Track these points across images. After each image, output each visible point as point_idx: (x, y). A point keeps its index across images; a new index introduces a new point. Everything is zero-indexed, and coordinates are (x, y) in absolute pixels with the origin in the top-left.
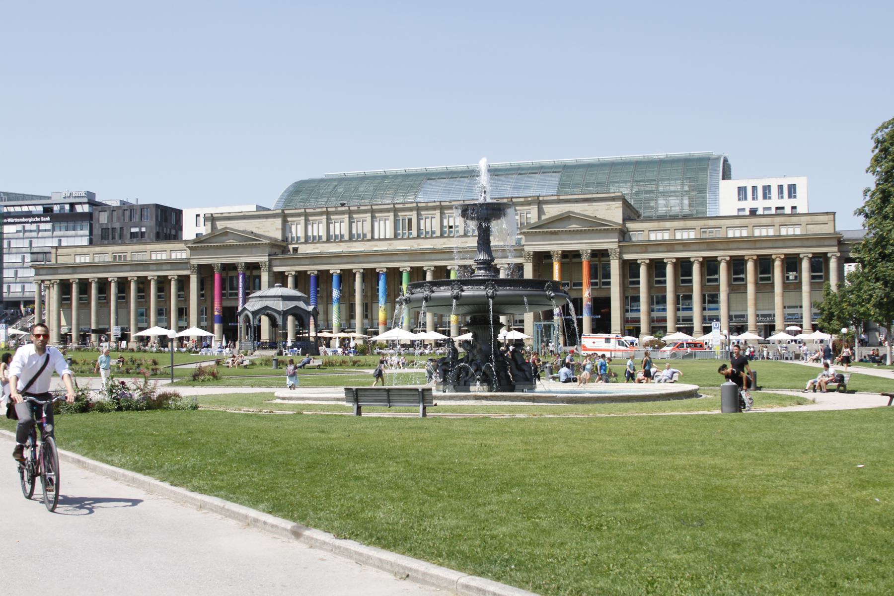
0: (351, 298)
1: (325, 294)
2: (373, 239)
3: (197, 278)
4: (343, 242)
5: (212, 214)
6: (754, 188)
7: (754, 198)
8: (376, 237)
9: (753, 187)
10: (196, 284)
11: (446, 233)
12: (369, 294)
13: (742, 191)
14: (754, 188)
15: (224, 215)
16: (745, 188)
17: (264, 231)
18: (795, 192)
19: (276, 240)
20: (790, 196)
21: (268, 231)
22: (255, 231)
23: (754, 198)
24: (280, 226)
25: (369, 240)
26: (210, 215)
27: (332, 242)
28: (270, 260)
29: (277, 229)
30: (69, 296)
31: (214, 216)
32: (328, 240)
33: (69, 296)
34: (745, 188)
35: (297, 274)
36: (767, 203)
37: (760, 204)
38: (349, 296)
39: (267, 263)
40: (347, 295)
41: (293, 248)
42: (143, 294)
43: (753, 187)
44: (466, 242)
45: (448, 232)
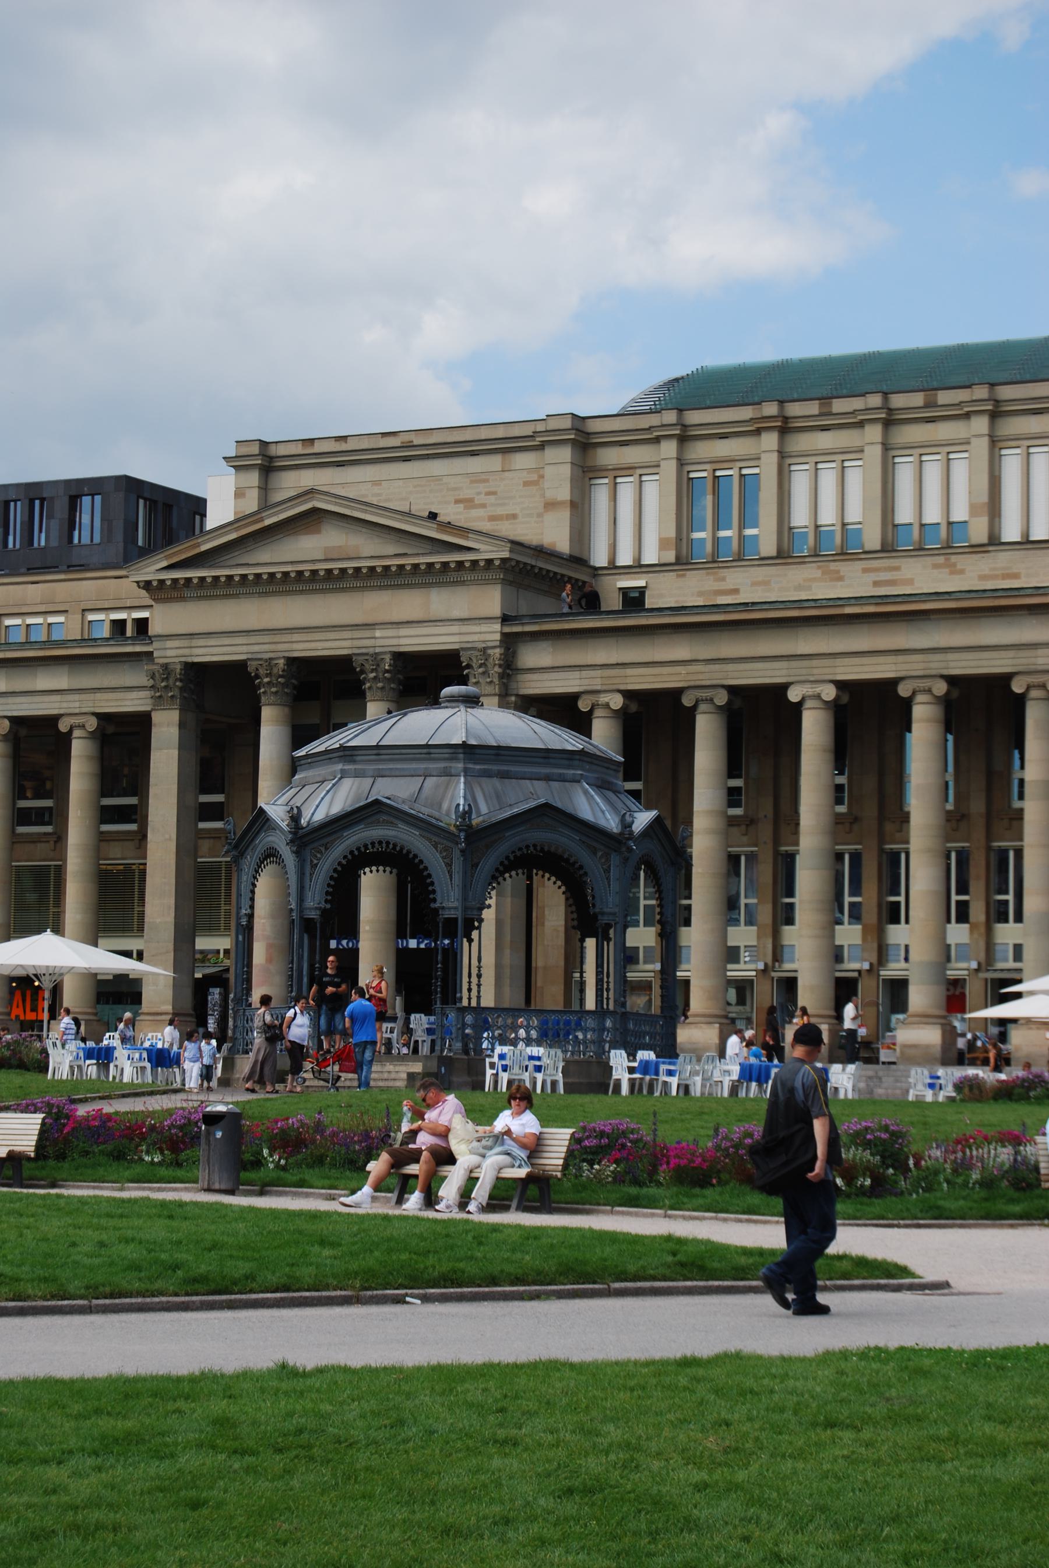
0: (889, 827)
1: (767, 809)
2: (994, 541)
3: (182, 725)
4: (854, 557)
5: (264, 444)
8: (1011, 532)
12: (977, 806)
15: (318, 448)
17: (493, 518)
19: (550, 554)
22: (449, 513)
24: (564, 493)
25: (977, 549)
26: (255, 449)
27: (801, 561)
28: (510, 642)
29: (551, 505)
30: (133, 801)
31: (273, 451)
32: (783, 555)
33: (133, 801)
35: (634, 708)
38: (882, 818)
40: (870, 810)
41: (625, 592)
42: (219, 798)
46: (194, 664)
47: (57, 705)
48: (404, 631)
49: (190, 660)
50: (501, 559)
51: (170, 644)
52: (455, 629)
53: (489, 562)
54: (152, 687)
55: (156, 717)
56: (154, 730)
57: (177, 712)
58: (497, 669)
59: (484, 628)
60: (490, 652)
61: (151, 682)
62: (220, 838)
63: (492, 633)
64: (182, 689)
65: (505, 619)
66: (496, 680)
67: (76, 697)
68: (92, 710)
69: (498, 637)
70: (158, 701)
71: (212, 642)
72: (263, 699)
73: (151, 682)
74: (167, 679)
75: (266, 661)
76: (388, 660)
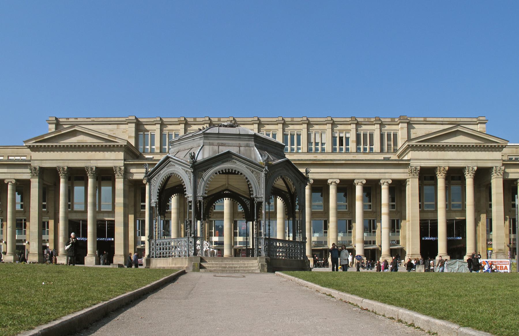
39: (123, 168)
46: (42, 167)
47: (4, 176)
49: (41, 166)
50: (124, 145)
52: (112, 162)
53: (121, 146)
54: (31, 172)
55: (32, 180)
56: (32, 184)
57: (38, 179)
58: (123, 172)
59: (119, 162)
60: (121, 167)
61: (31, 171)
62: (45, 213)
63: (121, 164)
64: (39, 173)
65: (125, 160)
66: (123, 175)
67: (9, 174)
68: (14, 178)
69: (123, 164)
70: (33, 176)
72: (61, 177)
73: (31, 171)
74: (35, 171)
75: (62, 167)
76: (95, 168)
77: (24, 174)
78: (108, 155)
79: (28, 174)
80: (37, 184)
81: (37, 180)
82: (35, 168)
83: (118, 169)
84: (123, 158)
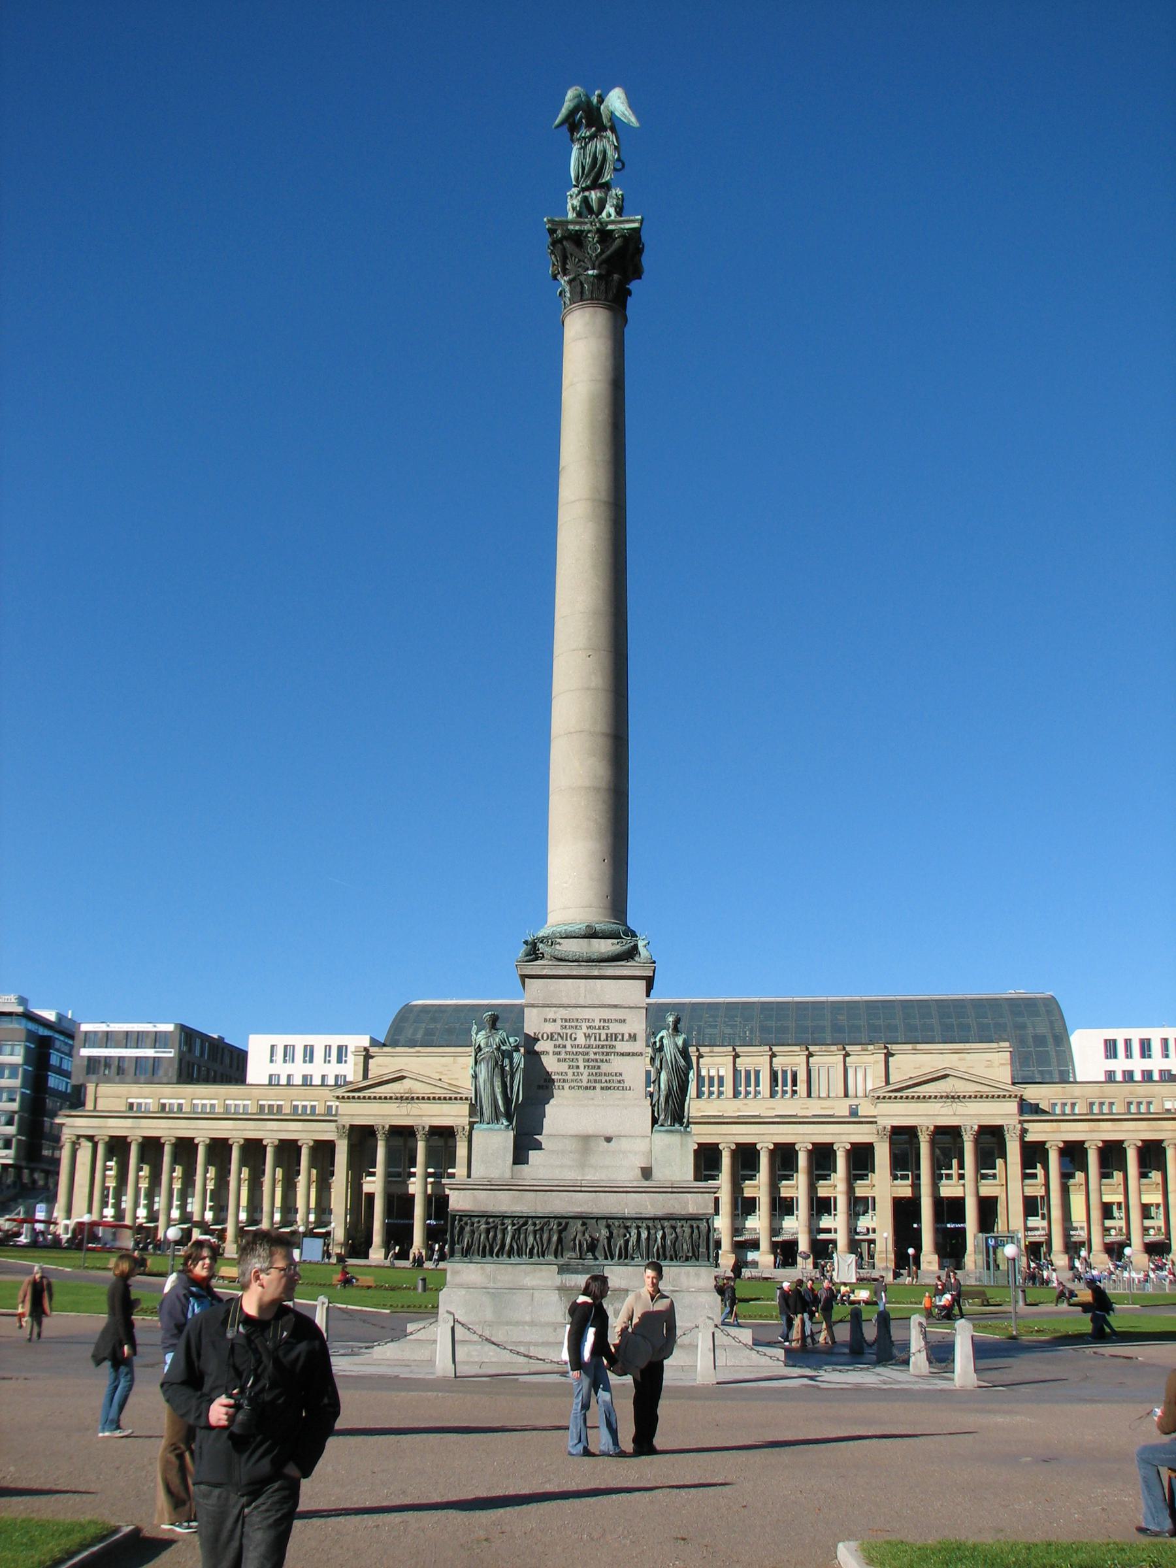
6: (1128, 1042)
7: (1129, 1055)
9: (1126, 1041)
10: (345, 1156)
11: (750, 1093)
13: (1110, 1049)
14: (1128, 1042)
16: (1114, 1041)
18: (1149, 1050)
20: (1143, 1056)
21: (457, 1079)
23: (1129, 1055)
34: (1114, 1041)
36: (1147, 1064)
37: (1138, 1065)
39: (467, 1128)
43: (1126, 1041)
44: (774, 1109)
45: (753, 1093)
48: (434, 1118)
51: (345, 1117)
52: (452, 1118)
59: (463, 1119)
63: (465, 1121)
70: (340, 1137)
71: (361, 1118)
77: (326, 1132)
78: (446, 1108)
79: (332, 1133)
80: (345, 1148)
81: (346, 1142)
82: (344, 1126)
83: (460, 1129)
84: (467, 1114)
